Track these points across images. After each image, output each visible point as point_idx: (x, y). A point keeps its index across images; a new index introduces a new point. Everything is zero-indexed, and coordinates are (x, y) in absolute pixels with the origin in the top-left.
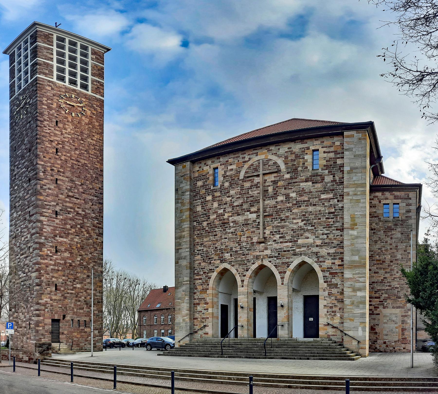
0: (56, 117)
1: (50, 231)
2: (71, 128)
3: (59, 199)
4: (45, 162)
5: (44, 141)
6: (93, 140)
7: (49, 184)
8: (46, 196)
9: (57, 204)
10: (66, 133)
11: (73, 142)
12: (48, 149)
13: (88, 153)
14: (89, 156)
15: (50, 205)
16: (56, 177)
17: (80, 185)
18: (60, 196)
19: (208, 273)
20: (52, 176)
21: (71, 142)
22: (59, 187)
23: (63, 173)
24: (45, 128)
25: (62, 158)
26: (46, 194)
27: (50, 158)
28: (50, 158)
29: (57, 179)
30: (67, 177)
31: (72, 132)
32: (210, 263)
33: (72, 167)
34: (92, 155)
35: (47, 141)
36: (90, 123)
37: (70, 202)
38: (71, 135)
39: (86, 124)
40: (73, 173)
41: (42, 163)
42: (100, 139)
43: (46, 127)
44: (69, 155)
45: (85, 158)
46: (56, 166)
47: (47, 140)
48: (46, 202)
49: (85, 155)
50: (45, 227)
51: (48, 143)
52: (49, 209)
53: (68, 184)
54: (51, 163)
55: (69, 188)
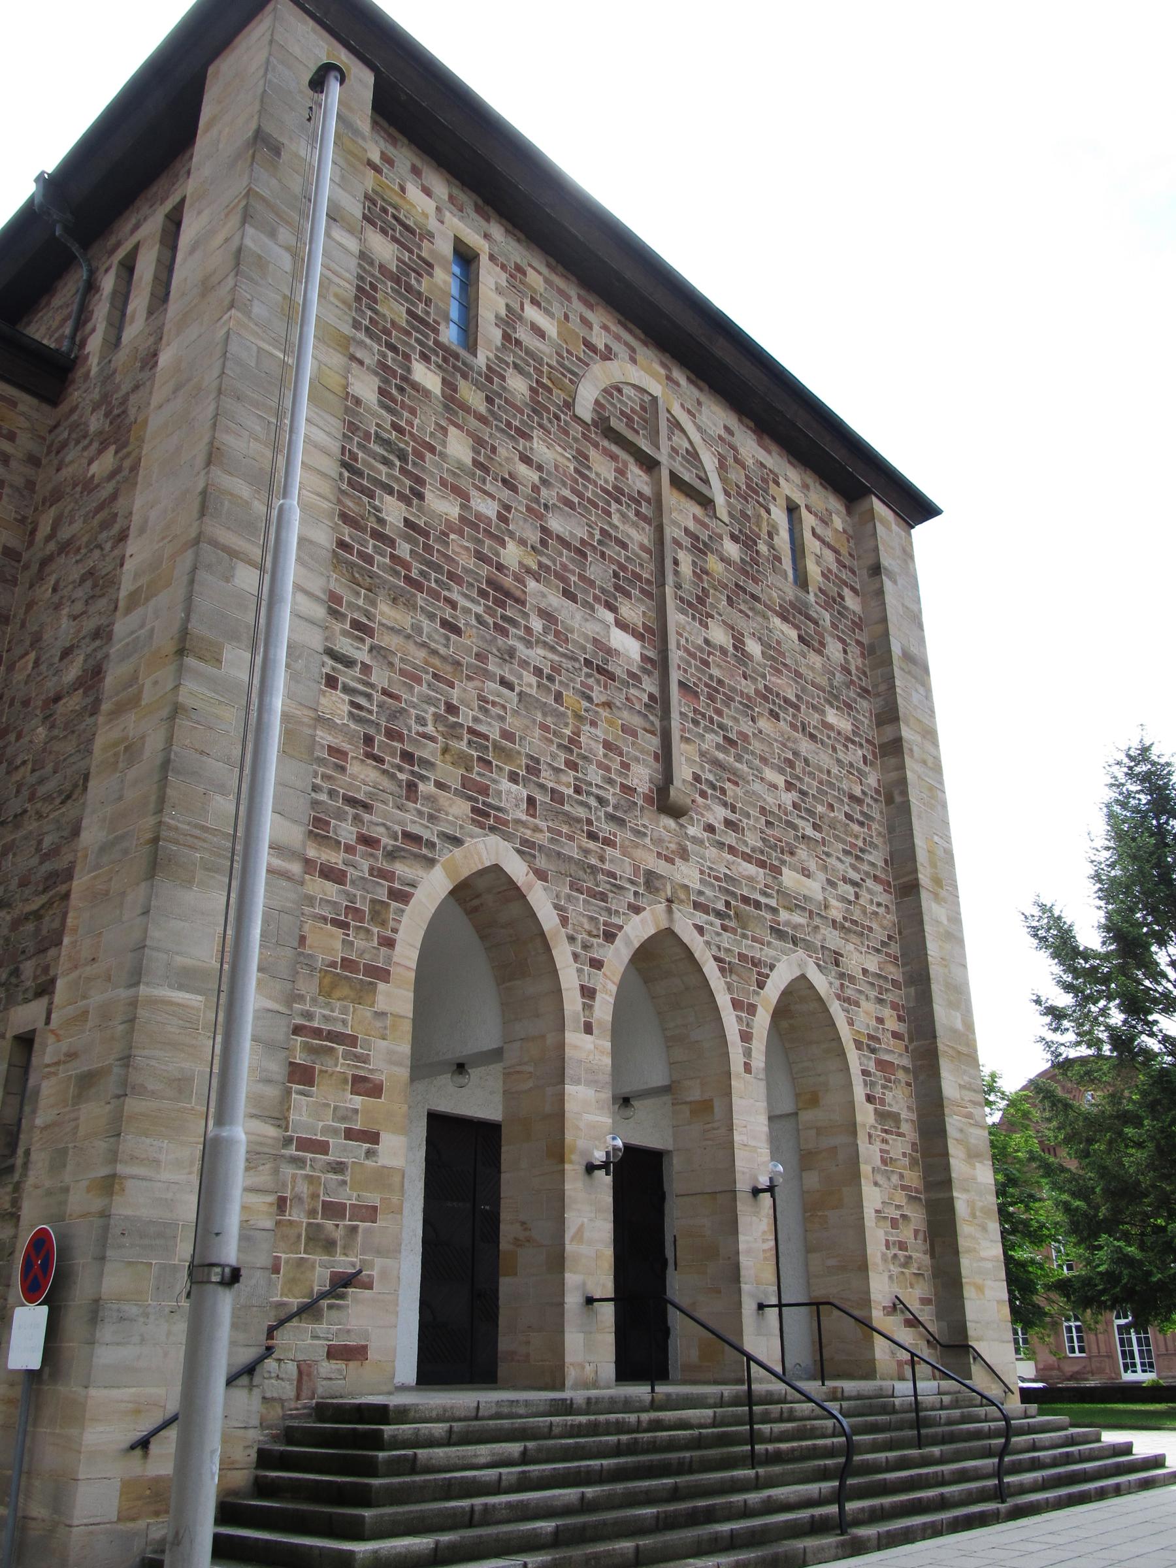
19: (392, 855)
32: (411, 787)
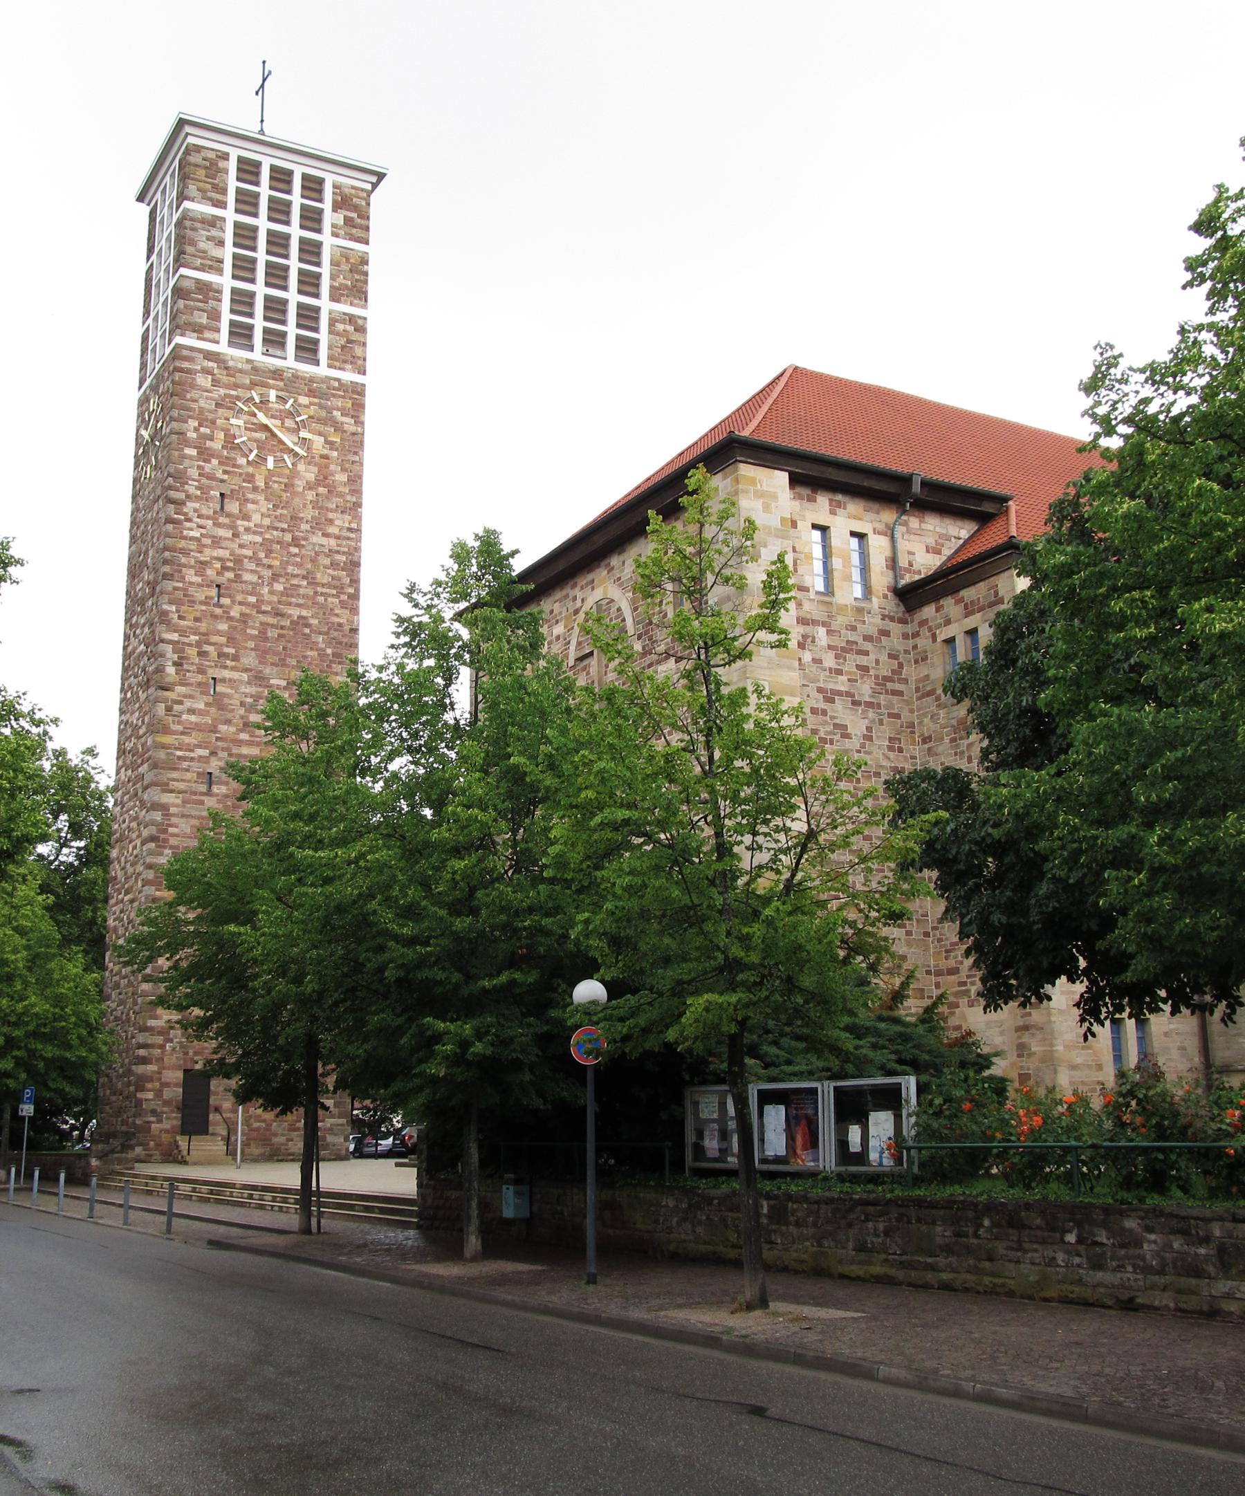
0: (222, 481)
1: (188, 831)
2: (264, 510)
3: (218, 739)
4: (183, 633)
5: (185, 566)
6: (325, 535)
7: (191, 697)
8: (182, 733)
9: (213, 753)
10: (247, 530)
11: (267, 557)
12: (191, 590)
13: (313, 583)
14: (316, 593)
15: (192, 759)
16: (213, 672)
17: (285, 688)
18: (223, 728)
20: (201, 671)
21: (262, 555)
22: (218, 702)
23: (235, 658)
24: (188, 525)
25: (232, 614)
26: (180, 728)
27: (197, 620)
28: (197, 620)
29: (214, 679)
30: (246, 670)
31: (267, 522)
33: (263, 633)
34: (323, 585)
35: (191, 567)
36: (323, 478)
37: (250, 744)
38: (261, 533)
39: (309, 486)
40: (262, 654)
41: (175, 637)
42: (350, 530)
43: (190, 520)
44: (252, 599)
45: (301, 601)
46: (215, 639)
47: (192, 562)
48: (181, 749)
49: (302, 591)
50: (174, 820)
51: (192, 572)
52: (187, 770)
53: (247, 691)
54: (200, 634)
55: (249, 700)
